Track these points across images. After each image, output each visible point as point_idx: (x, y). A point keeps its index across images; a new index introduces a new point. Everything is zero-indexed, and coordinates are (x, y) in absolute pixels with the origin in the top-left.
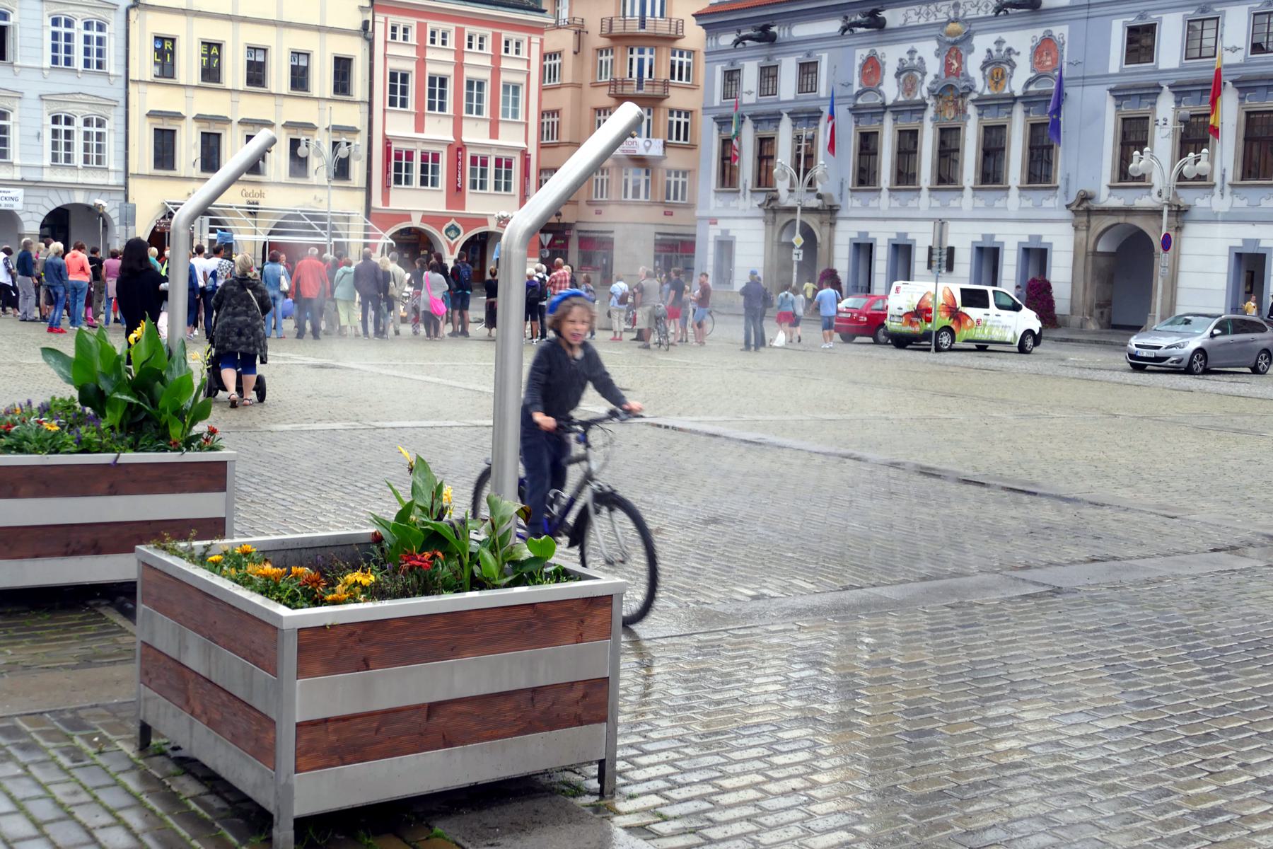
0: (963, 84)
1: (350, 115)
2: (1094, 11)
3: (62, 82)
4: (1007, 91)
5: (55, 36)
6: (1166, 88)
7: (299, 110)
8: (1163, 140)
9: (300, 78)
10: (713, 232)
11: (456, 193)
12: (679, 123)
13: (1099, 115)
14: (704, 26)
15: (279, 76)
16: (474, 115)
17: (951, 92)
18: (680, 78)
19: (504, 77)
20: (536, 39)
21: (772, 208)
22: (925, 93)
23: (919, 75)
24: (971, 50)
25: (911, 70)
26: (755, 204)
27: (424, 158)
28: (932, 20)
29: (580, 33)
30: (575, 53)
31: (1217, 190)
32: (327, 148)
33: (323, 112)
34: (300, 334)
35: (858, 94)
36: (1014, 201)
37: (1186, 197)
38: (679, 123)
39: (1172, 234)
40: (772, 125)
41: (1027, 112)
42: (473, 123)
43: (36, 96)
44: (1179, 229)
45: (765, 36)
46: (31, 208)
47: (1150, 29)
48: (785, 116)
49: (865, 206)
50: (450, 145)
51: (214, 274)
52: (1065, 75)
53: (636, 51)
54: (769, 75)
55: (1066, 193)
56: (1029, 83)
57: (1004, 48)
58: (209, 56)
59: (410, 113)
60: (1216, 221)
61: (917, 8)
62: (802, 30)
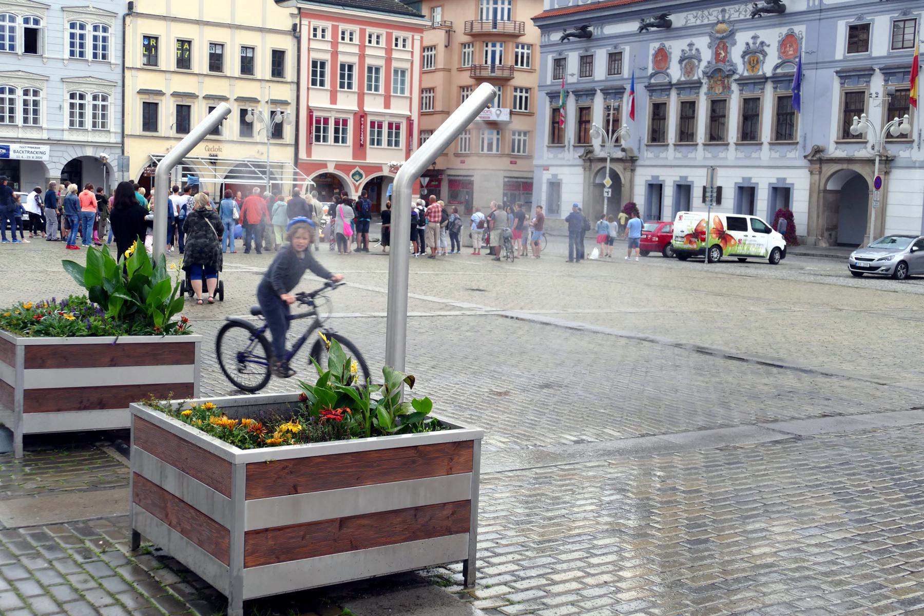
0: (729, 68)
1: (284, 92)
2: (824, 15)
3: (77, 69)
4: (760, 73)
5: (72, 36)
6: (878, 71)
7: (247, 89)
8: (875, 109)
9: (247, 66)
10: (546, 176)
11: (360, 148)
12: (521, 97)
13: (828, 90)
14: (539, 27)
15: (232, 64)
16: (373, 92)
17: (720, 74)
18: (522, 65)
19: (395, 64)
20: (417, 37)
21: (589, 159)
22: (701, 75)
23: (696, 62)
24: (734, 43)
25: (691, 58)
26: (577, 155)
27: (337, 123)
28: (706, 22)
29: (449, 32)
30: (446, 46)
31: (915, 145)
32: (266, 116)
33: (264, 90)
34: (247, 250)
35: (652, 76)
36: (765, 153)
37: (892, 150)
38: (521, 97)
39: (882, 177)
40: (589, 98)
41: (775, 88)
42: (371, 98)
43: (59, 79)
44: (887, 173)
45: (583, 34)
46: (55, 159)
47: (866, 28)
49: (657, 157)
50: (355, 114)
51: (184, 207)
52: (803, 61)
53: (490, 45)
54: (586, 62)
55: (804, 147)
56: (776, 67)
57: (758, 41)
58: (182, 49)
59: (326, 90)
60: (915, 168)
61: (694, 13)
62: (611, 29)
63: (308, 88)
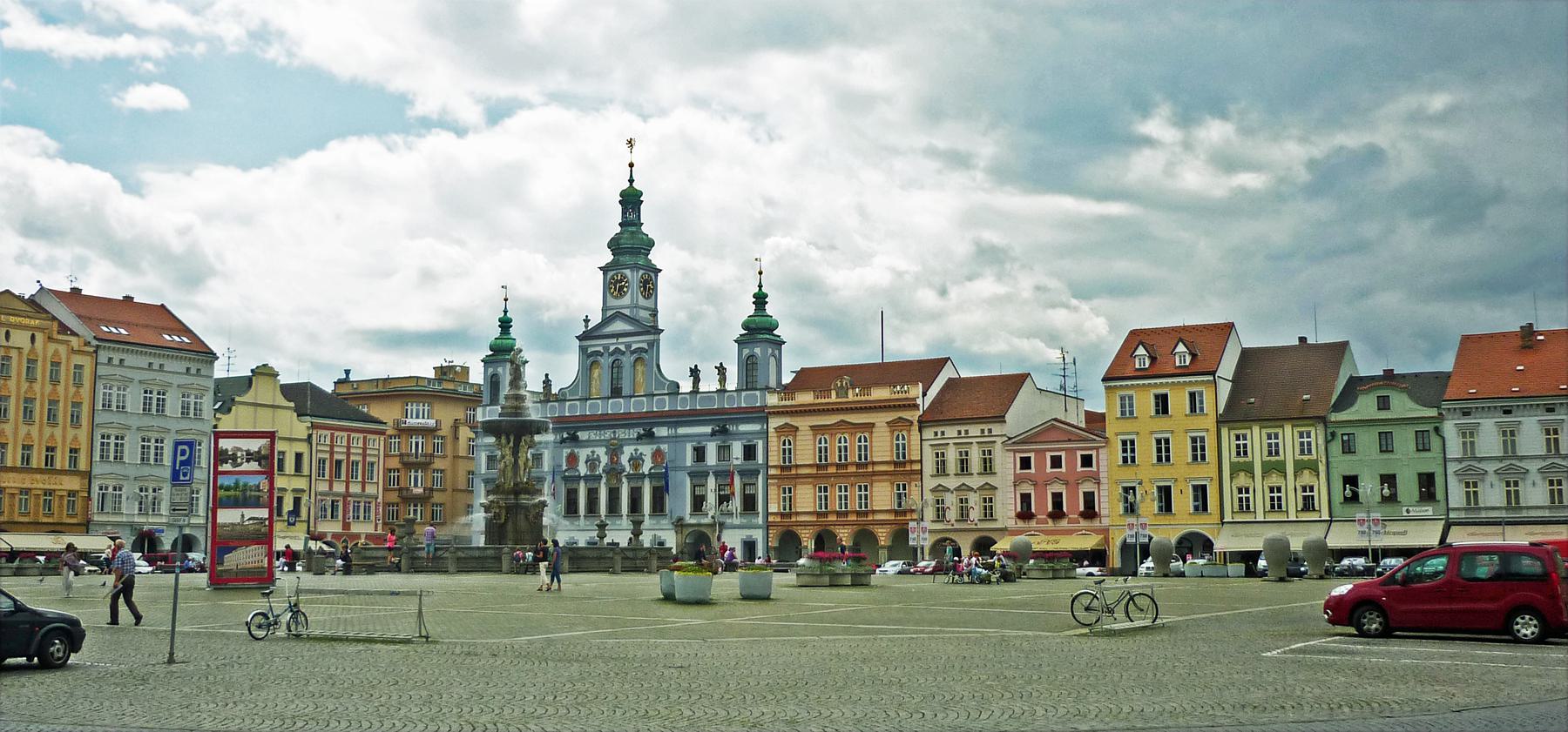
1: (301, 483)
8: (711, 499)
11: (346, 526)
13: (683, 484)
17: (614, 471)
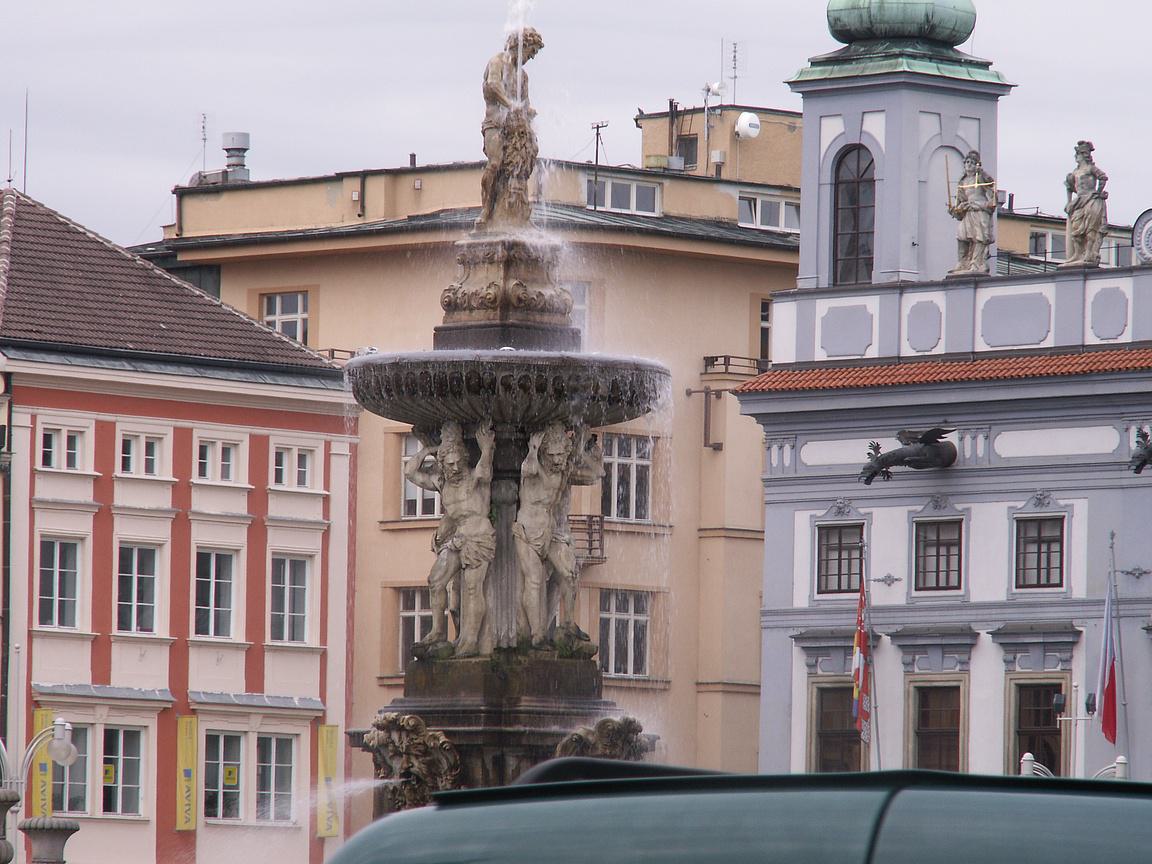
14: (758, 416)
16: (211, 637)
19: (278, 542)
38: (622, 625)
45: (931, 457)
48: (985, 638)
54: (939, 540)
62: (1017, 444)
63: (31, 635)
